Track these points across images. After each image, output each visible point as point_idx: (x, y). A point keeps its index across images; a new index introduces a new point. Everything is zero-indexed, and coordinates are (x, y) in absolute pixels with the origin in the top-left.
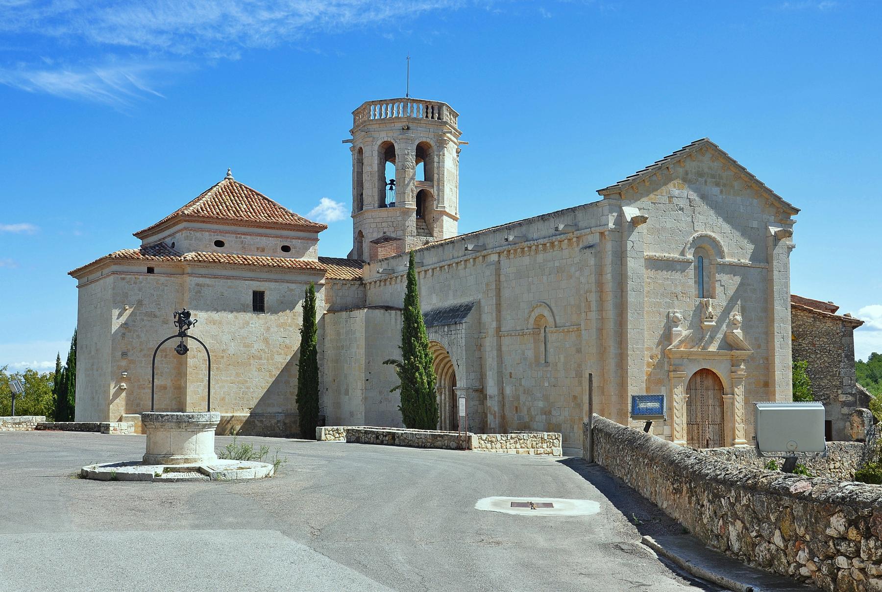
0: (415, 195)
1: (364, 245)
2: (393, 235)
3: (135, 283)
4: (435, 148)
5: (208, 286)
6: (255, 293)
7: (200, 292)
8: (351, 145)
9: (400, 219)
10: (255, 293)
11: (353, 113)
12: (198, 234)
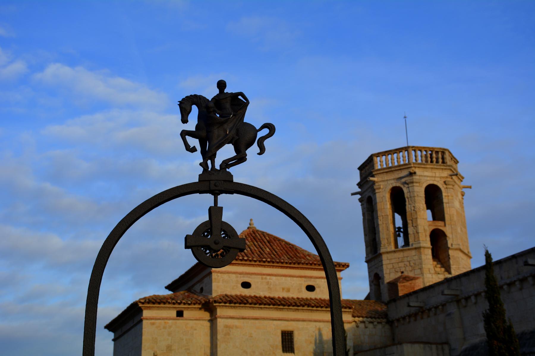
0: (428, 234)
1: (382, 287)
2: (411, 274)
3: (165, 328)
4: (443, 189)
5: (237, 327)
7: (228, 334)
8: (359, 196)
9: (416, 258)
11: (359, 169)
12: (225, 276)
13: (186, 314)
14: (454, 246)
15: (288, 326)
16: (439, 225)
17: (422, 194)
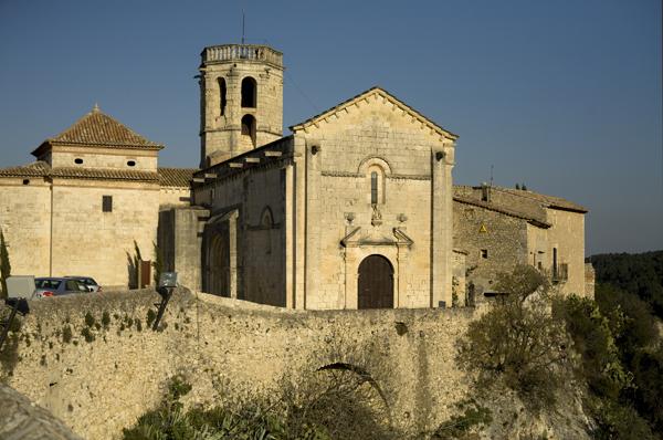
4: (258, 82)
5: (67, 193)
6: (105, 197)
10: (105, 197)
12: (62, 154)
13: (32, 182)
15: (108, 192)
16: (249, 111)
17: (240, 86)
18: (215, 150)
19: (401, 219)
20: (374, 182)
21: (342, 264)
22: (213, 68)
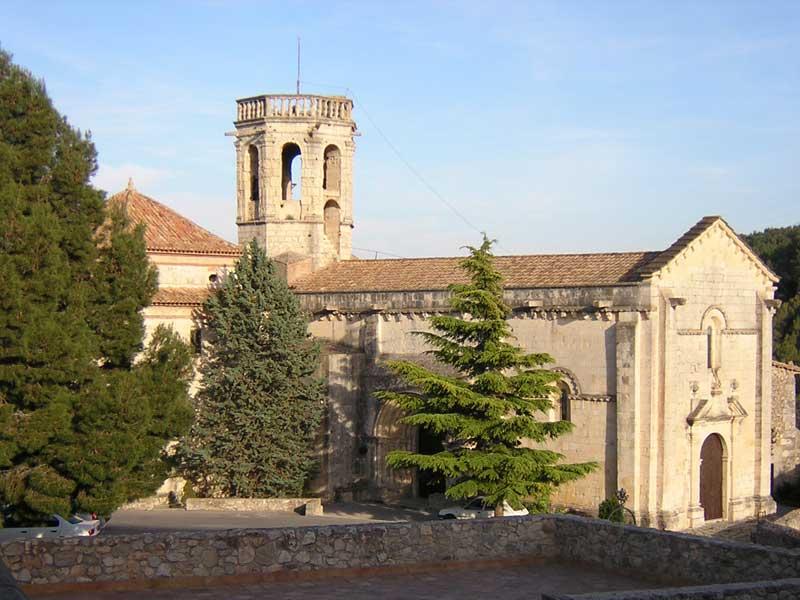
14: (347, 221)
18: (282, 251)
19: (734, 385)
20: (709, 337)
21: (688, 448)
22: (275, 126)
